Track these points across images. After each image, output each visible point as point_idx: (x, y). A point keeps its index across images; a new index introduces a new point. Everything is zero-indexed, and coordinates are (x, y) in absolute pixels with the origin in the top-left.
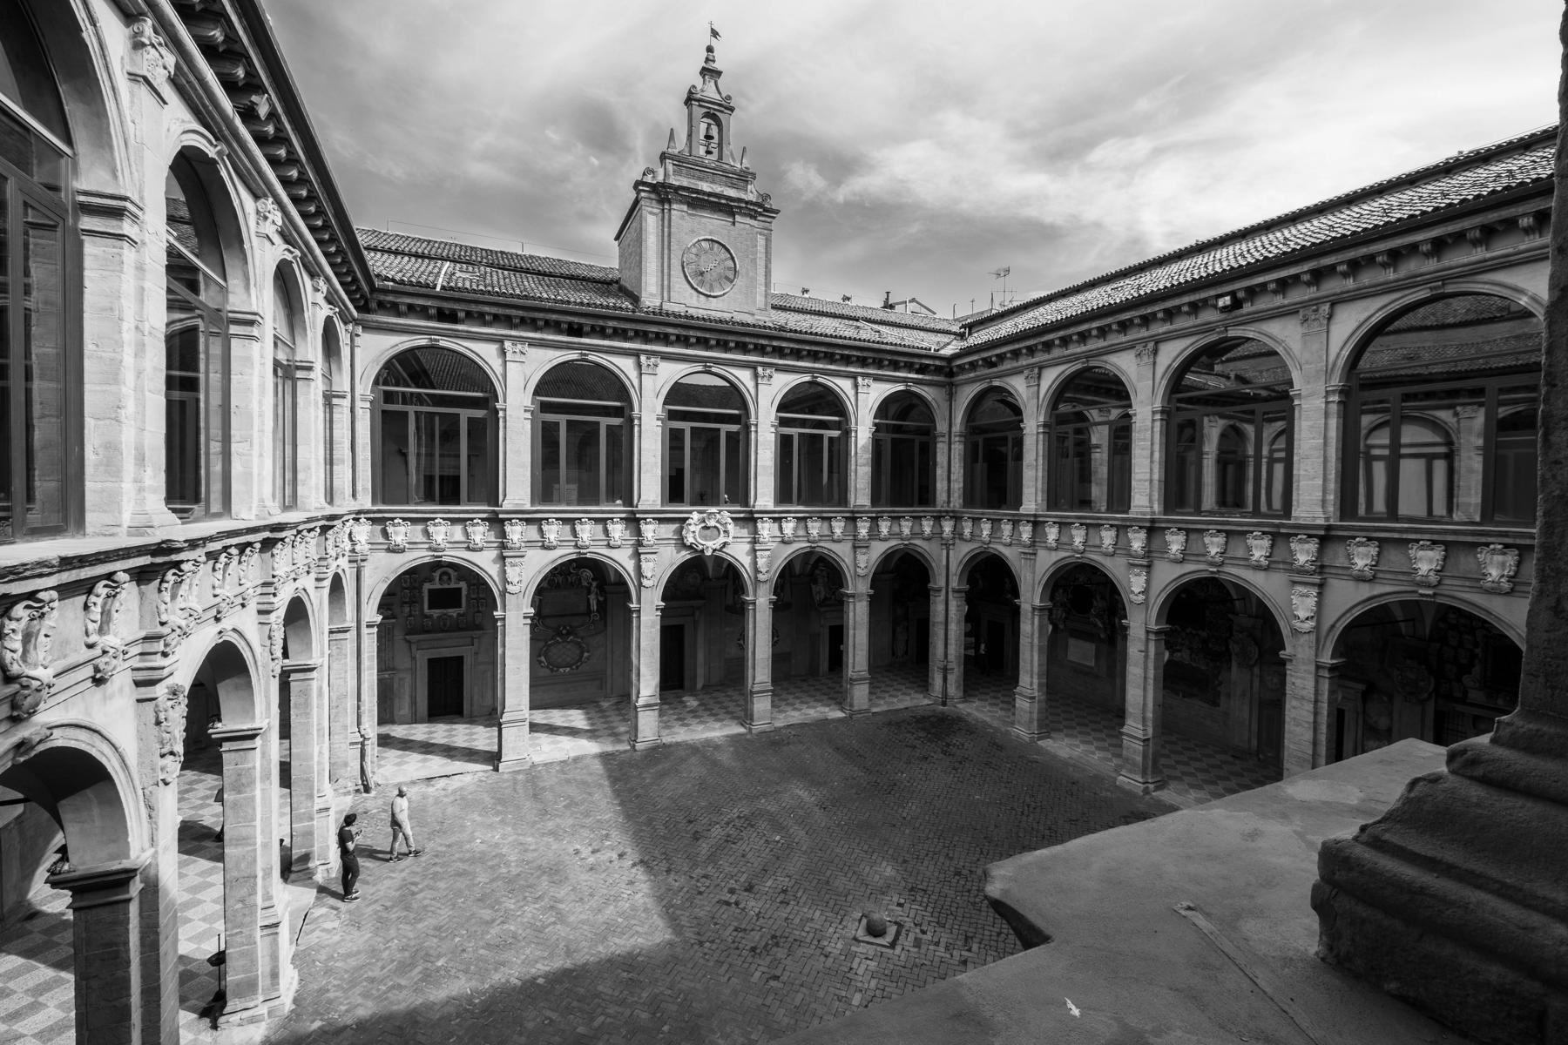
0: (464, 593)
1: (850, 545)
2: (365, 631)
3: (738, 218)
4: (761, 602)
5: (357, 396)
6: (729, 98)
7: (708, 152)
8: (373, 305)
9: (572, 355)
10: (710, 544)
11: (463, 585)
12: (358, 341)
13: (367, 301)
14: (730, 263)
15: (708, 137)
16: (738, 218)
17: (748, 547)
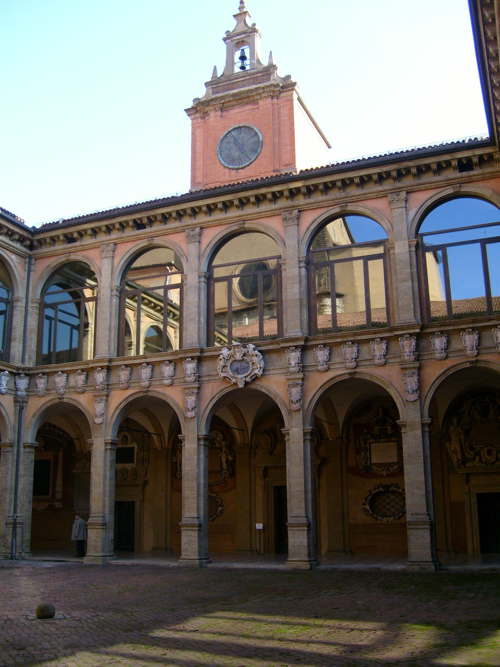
0: (136, 451)
1: (397, 368)
2: (22, 449)
3: (261, 103)
4: (295, 431)
5: (30, 300)
6: (254, 25)
7: (243, 68)
8: (35, 243)
9: (143, 243)
10: (240, 376)
11: (135, 445)
12: (33, 267)
13: (32, 242)
14: (255, 139)
15: (243, 58)
16: (261, 103)
17: (283, 378)
